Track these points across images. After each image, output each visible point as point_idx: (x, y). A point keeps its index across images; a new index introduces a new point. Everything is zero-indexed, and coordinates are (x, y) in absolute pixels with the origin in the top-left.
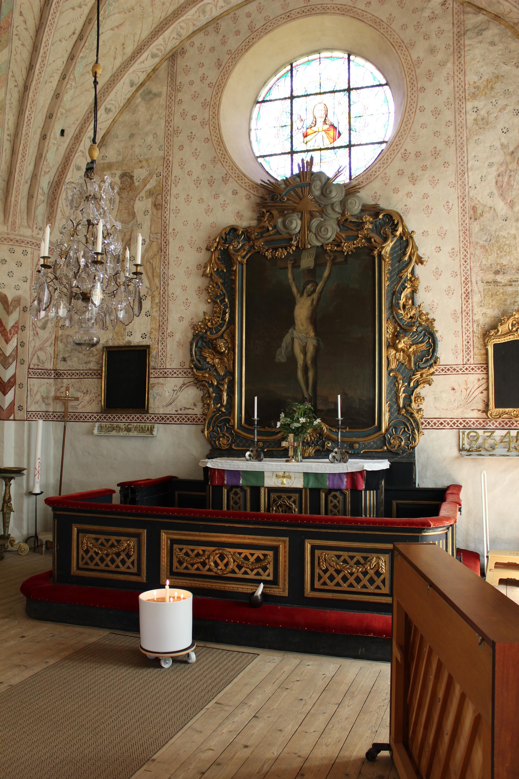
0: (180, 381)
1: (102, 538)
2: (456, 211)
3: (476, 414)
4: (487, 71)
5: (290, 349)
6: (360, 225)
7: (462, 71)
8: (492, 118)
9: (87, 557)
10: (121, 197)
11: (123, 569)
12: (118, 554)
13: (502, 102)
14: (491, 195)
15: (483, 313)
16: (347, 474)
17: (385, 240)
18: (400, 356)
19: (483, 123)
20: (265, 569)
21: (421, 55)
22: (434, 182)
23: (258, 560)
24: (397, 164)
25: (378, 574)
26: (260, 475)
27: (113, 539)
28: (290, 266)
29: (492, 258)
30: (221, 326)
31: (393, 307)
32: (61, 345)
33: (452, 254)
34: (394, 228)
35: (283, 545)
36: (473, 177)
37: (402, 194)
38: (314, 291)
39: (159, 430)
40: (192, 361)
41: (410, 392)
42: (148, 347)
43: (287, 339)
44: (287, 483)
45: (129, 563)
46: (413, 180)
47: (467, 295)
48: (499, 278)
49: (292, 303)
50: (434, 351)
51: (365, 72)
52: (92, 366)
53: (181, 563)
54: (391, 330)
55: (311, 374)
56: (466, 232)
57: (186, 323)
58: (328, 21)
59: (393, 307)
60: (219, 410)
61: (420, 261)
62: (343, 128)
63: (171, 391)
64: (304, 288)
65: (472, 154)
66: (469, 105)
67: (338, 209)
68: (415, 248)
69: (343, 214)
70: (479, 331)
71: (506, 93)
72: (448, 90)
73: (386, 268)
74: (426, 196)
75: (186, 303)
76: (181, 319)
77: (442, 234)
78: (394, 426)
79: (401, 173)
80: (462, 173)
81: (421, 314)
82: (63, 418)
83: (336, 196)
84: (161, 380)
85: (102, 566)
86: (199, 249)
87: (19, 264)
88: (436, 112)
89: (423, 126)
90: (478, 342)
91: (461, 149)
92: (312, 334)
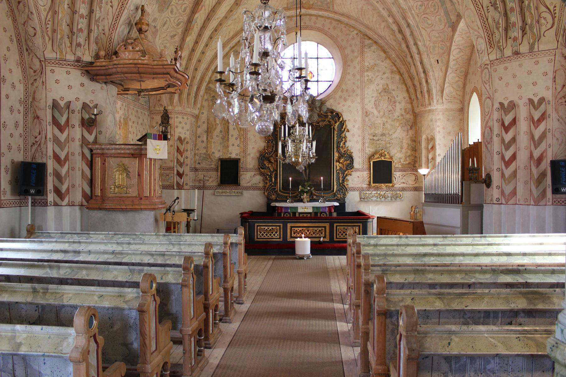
0: (253, 173)
1: (266, 228)
2: (360, 113)
3: (366, 186)
4: (372, 62)
6: (326, 116)
7: (363, 61)
8: (373, 79)
9: (261, 235)
11: (274, 237)
12: (272, 233)
13: (377, 74)
14: (372, 108)
15: (369, 150)
16: (328, 207)
17: (336, 122)
18: (341, 165)
19: (370, 81)
20: (322, 233)
21: (349, 52)
22: (353, 102)
23: (320, 231)
24: (340, 93)
25: (356, 232)
26: (296, 208)
27: (270, 228)
29: (372, 131)
30: (272, 152)
31: (338, 147)
32: (197, 157)
33: (359, 129)
34: (339, 118)
35: (327, 225)
36: (366, 101)
37: (341, 105)
39: (245, 192)
40: (259, 165)
41: (344, 178)
42: (240, 159)
44: (306, 211)
45: (276, 235)
46: (345, 100)
47: (364, 144)
48: (375, 138)
50: (353, 163)
51: (324, 52)
52: (213, 166)
53: (294, 233)
54: (337, 155)
55: (307, 171)
56: (364, 121)
57: (255, 150)
58: (313, 33)
59: (338, 147)
60: (271, 184)
61: (348, 131)
62: (315, 73)
63: (249, 177)
65: (366, 92)
66: (366, 74)
67: (318, 109)
68: (346, 126)
69: (320, 111)
70: (367, 157)
71: (378, 71)
72: (358, 68)
73: (336, 133)
74: (349, 107)
75: (255, 142)
76: (253, 148)
77: (355, 121)
78: (338, 190)
79: (341, 97)
80: (363, 99)
81: (348, 150)
82: (202, 187)
83: (318, 104)
84: (245, 173)
85: (266, 237)
87: (186, 124)
88: (354, 75)
89: (349, 80)
90: (367, 160)
91: (362, 90)
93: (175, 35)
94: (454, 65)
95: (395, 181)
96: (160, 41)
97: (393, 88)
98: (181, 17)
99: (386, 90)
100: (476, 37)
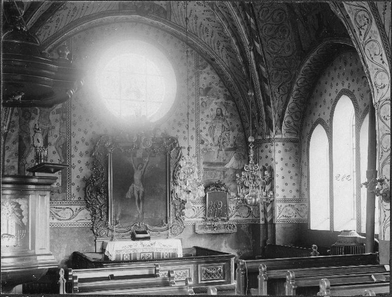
5: (132, 192)
10: (41, 111)
28: (132, 156)
36: (201, 128)
38: (142, 168)
43: (131, 188)
49: (133, 173)
56: (197, 148)
64: (138, 166)
80: (197, 125)
86: (87, 144)
92: (142, 186)
94: (296, 95)
95: (230, 215)
97: (227, 114)
99: (219, 116)
100: (377, 71)
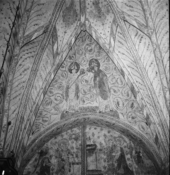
93: (133, 104)
96: (125, 116)
98: (124, 89)
